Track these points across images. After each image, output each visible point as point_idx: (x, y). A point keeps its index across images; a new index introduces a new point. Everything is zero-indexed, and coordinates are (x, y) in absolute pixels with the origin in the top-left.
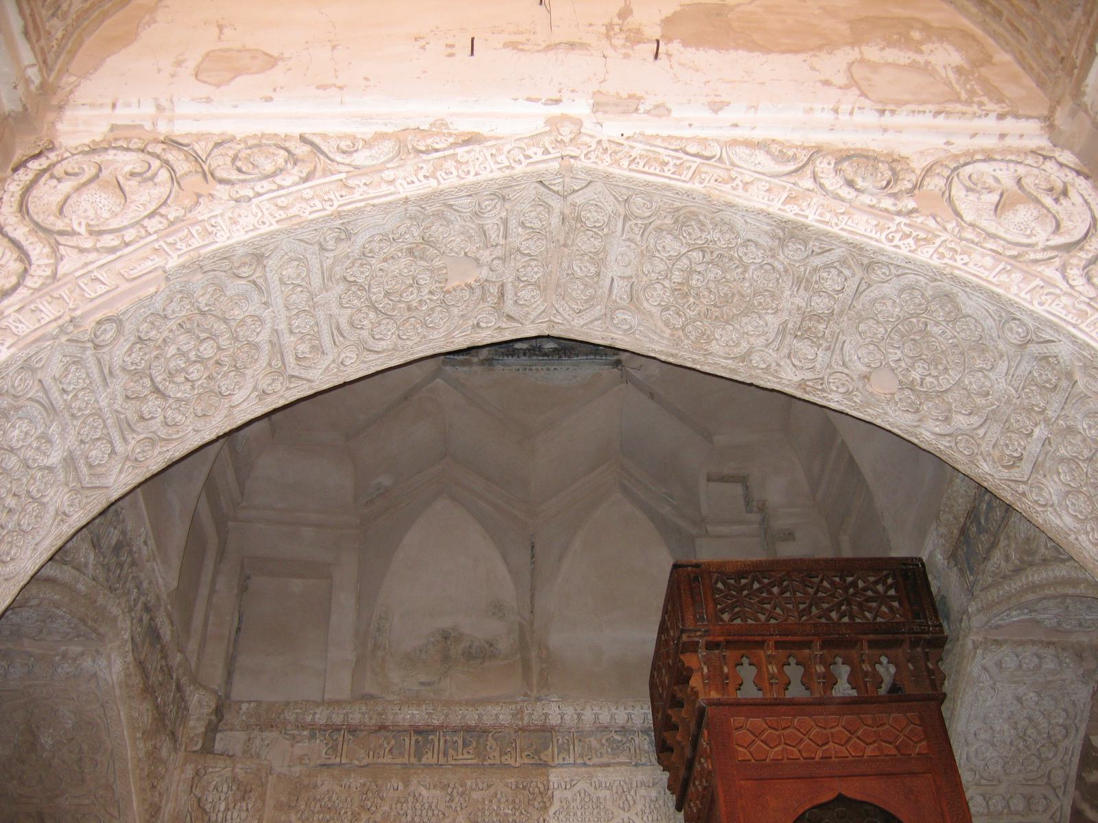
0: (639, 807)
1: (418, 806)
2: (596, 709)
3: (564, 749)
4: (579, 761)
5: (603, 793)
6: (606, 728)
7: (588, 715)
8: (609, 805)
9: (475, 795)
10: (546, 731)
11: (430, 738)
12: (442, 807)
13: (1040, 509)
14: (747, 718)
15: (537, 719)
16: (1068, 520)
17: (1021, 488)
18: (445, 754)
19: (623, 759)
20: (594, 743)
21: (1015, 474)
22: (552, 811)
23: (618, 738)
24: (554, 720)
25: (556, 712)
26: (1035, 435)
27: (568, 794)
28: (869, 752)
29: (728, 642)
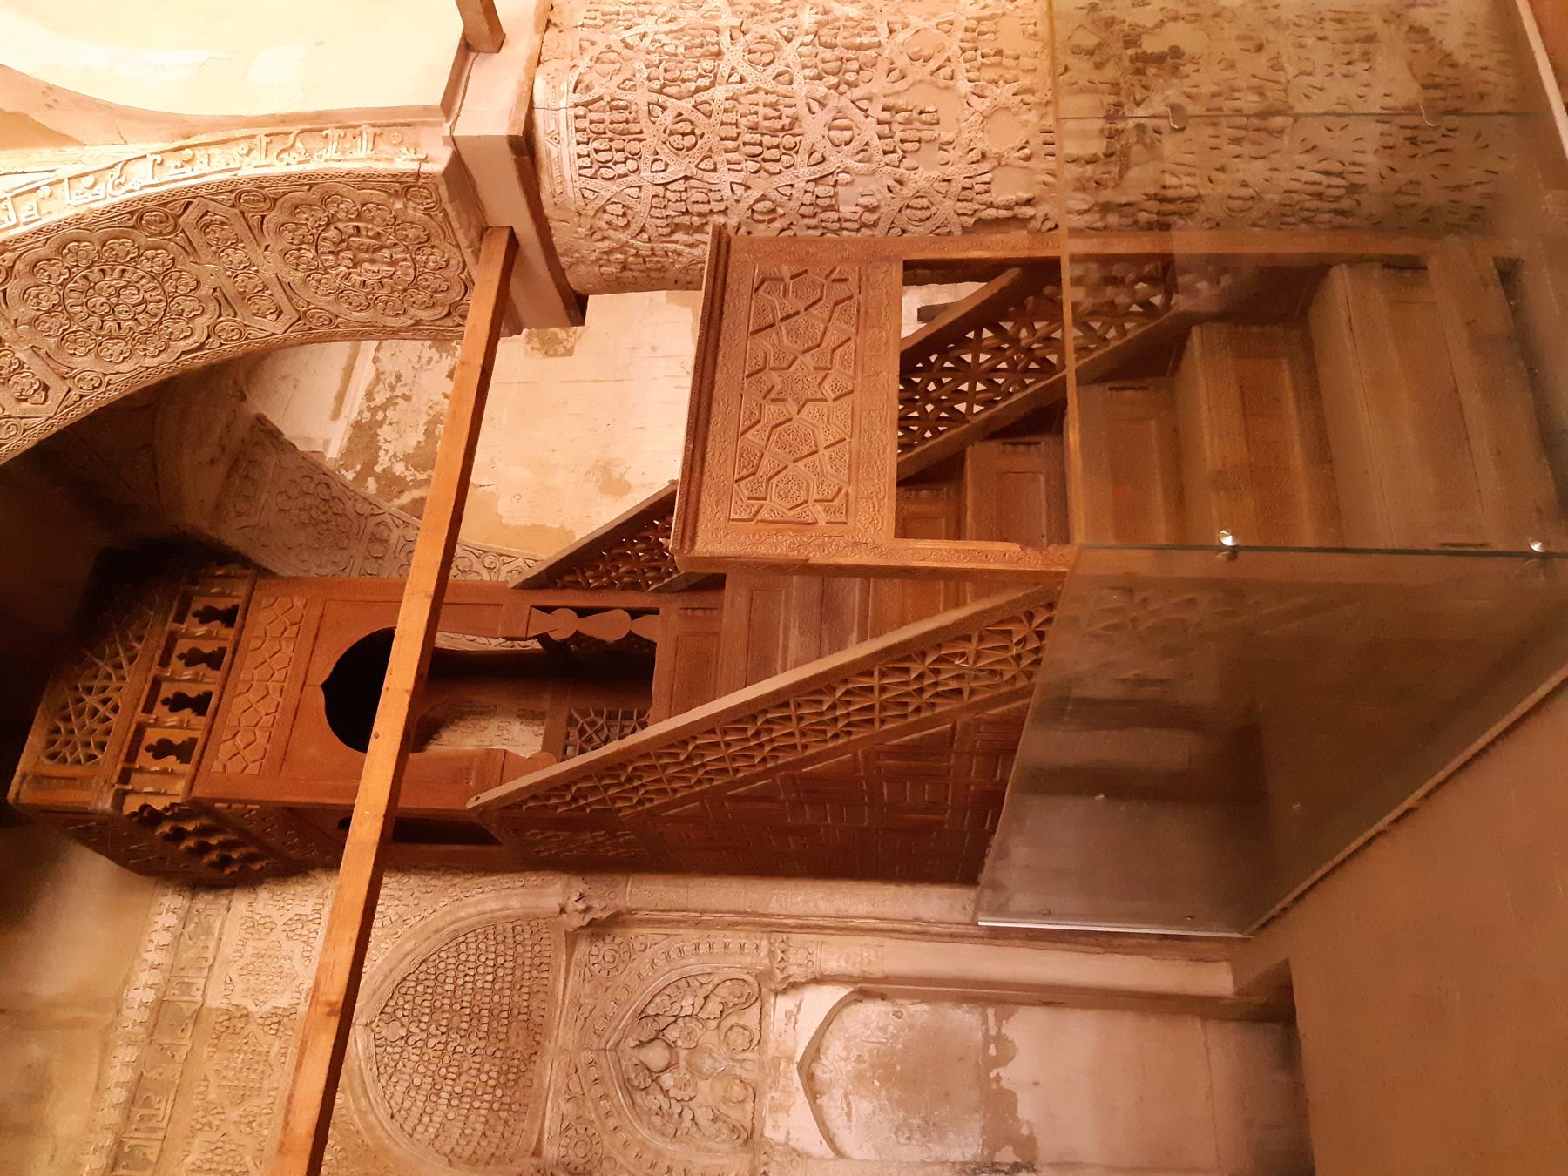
0: (275, 913)
1: (207, 1166)
2: (152, 947)
3: (186, 987)
4: (205, 972)
5: (249, 950)
6: (178, 939)
7: (155, 957)
8: (263, 944)
9: (212, 1097)
10: (160, 1007)
11: (126, 1149)
12: (215, 1136)
13: (102, 389)
14: (217, 757)
15: (145, 1015)
16: (125, 367)
17: (74, 395)
18: (154, 1130)
19: (217, 925)
20: (191, 954)
21: (57, 393)
22: (252, 1008)
23: (191, 927)
24: (150, 996)
25: (140, 995)
26: (24, 359)
27: (239, 987)
28: (288, 650)
29: (126, 760)
